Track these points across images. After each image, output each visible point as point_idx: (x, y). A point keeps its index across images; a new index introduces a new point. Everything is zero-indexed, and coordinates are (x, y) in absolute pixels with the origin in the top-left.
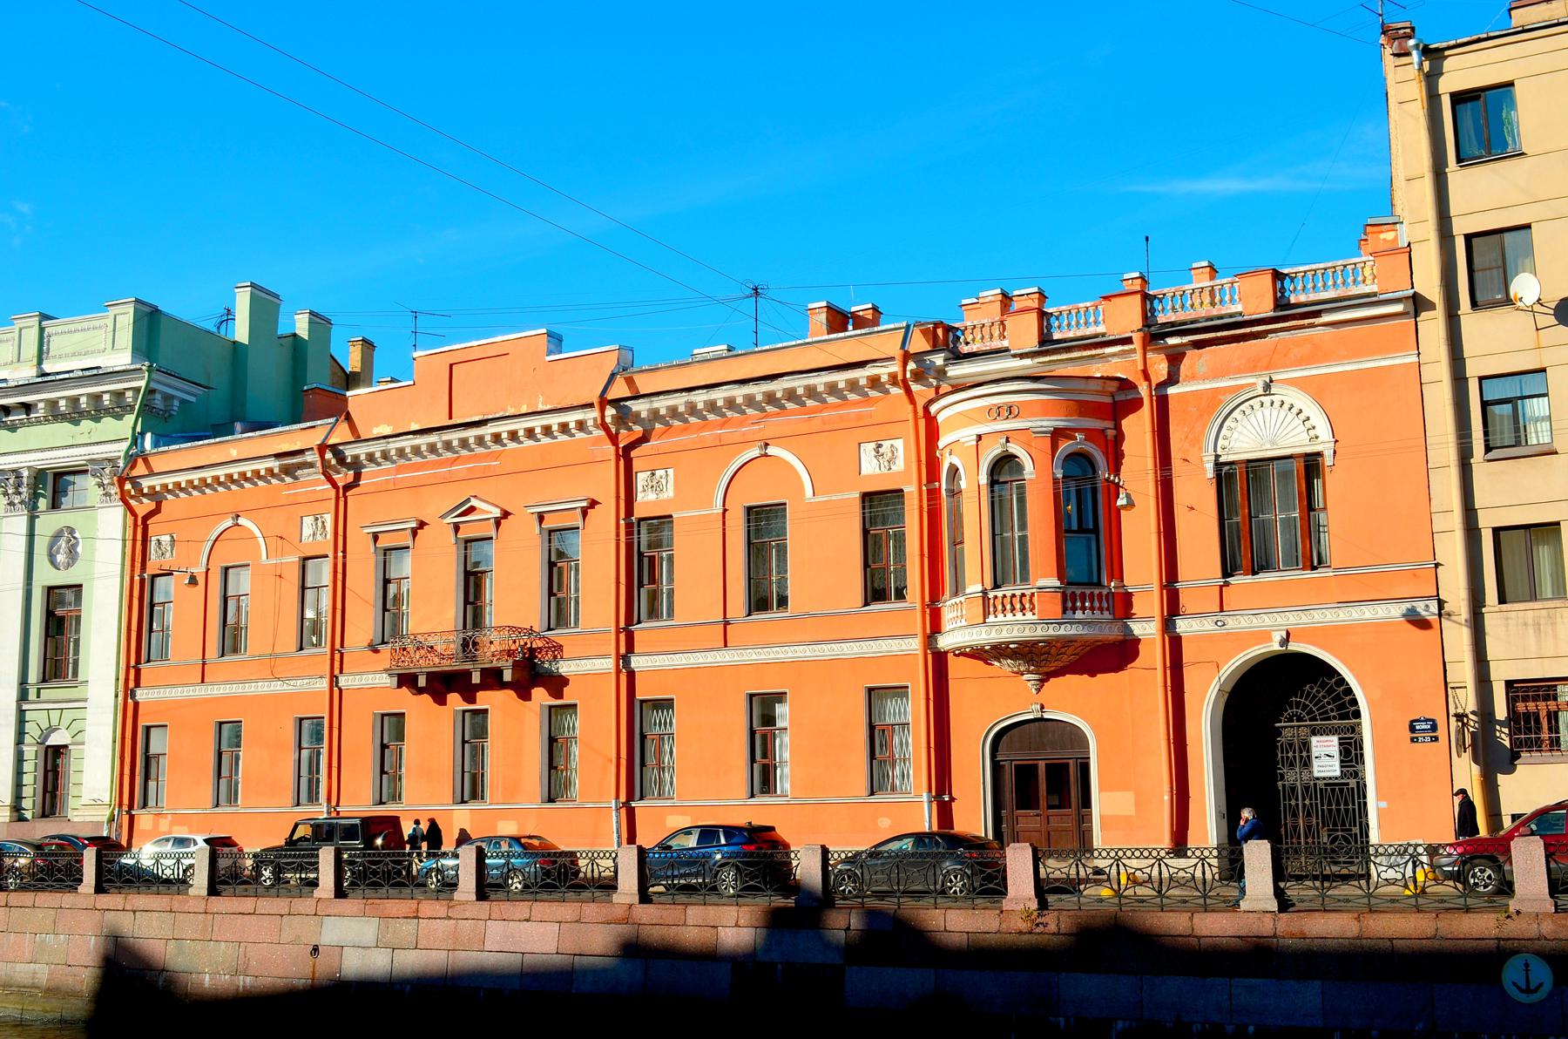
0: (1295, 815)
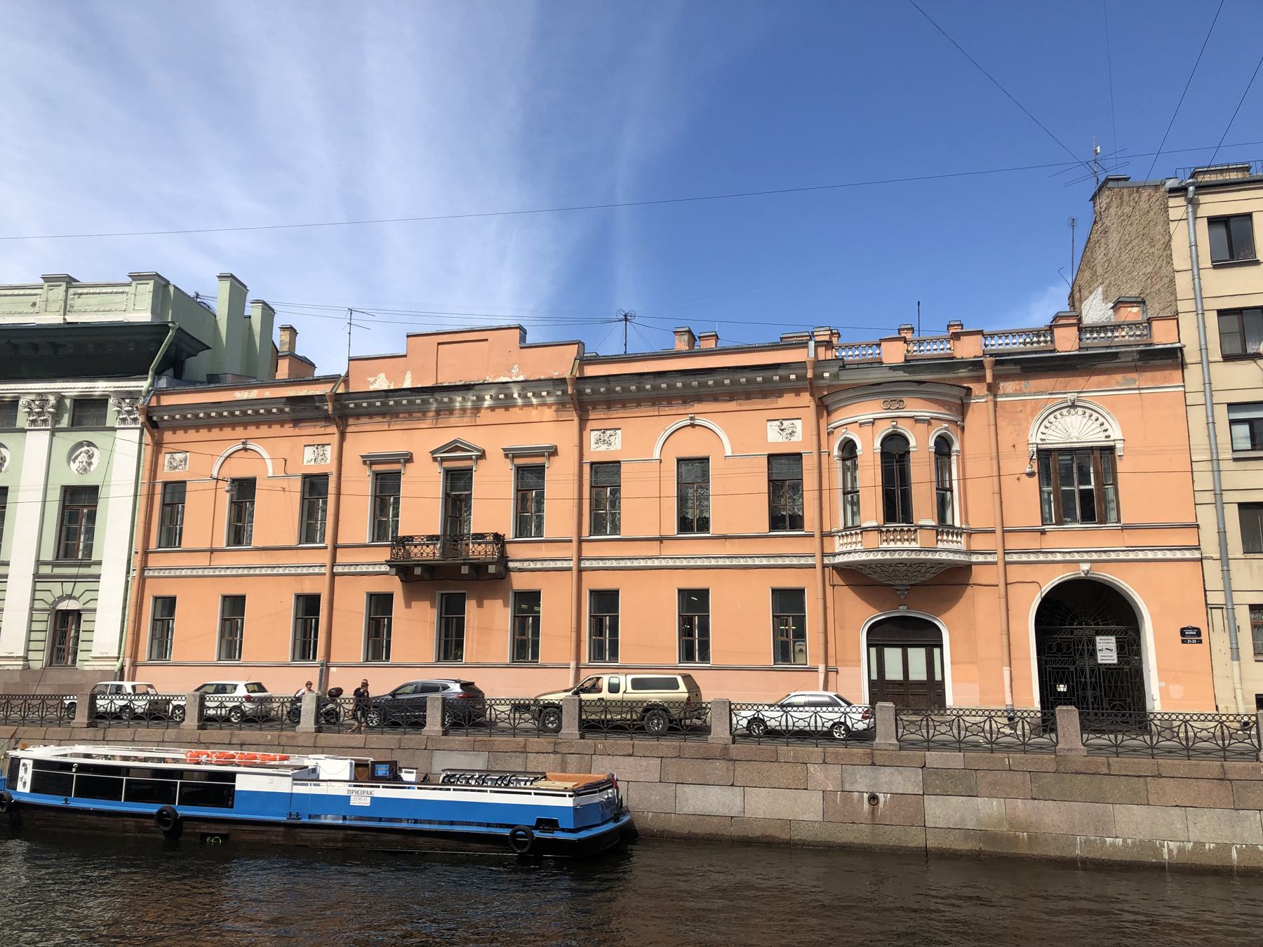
0: (1084, 689)
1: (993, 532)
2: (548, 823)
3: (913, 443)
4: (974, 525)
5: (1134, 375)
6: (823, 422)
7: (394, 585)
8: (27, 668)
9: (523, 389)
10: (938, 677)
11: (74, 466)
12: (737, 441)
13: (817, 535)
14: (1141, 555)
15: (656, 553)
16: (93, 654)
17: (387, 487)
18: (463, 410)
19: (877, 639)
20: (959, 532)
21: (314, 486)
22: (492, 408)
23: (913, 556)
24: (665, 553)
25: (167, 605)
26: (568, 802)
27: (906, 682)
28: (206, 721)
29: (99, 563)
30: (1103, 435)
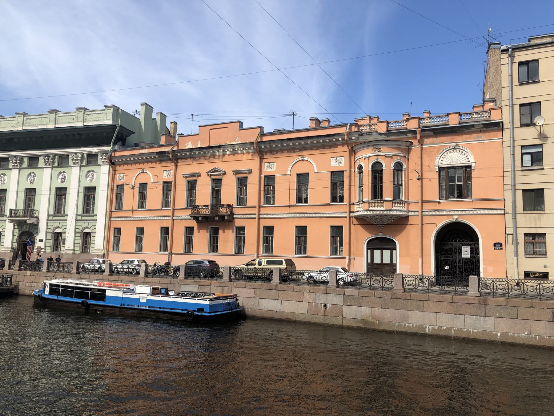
0: (456, 268)
1: (418, 202)
2: (201, 310)
3: (384, 166)
4: (411, 199)
5: (482, 134)
6: (353, 158)
7: (194, 224)
8: (74, 253)
10: (394, 262)
11: (88, 179)
12: (320, 165)
13: (348, 204)
14: (479, 212)
15: (287, 212)
16: (66, 248)
17: (192, 186)
18: (219, 156)
19: (371, 247)
20: (403, 203)
21: (167, 185)
22: (229, 155)
23: (382, 213)
24: (291, 212)
25: (118, 231)
26: (207, 302)
27: (382, 264)
28: (111, 272)
29: (96, 215)
30: (467, 161)
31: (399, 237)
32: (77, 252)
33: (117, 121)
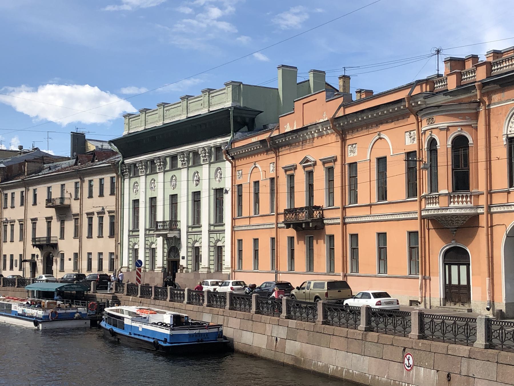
3: (438, 144)
7: (292, 232)
9: (322, 126)
18: (310, 139)
22: (318, 137)
23: (436, 213)
24: (373, 213)
29: (224, 225)
31: (471, 245)
32: (212, 271)
33: (239, 101)
